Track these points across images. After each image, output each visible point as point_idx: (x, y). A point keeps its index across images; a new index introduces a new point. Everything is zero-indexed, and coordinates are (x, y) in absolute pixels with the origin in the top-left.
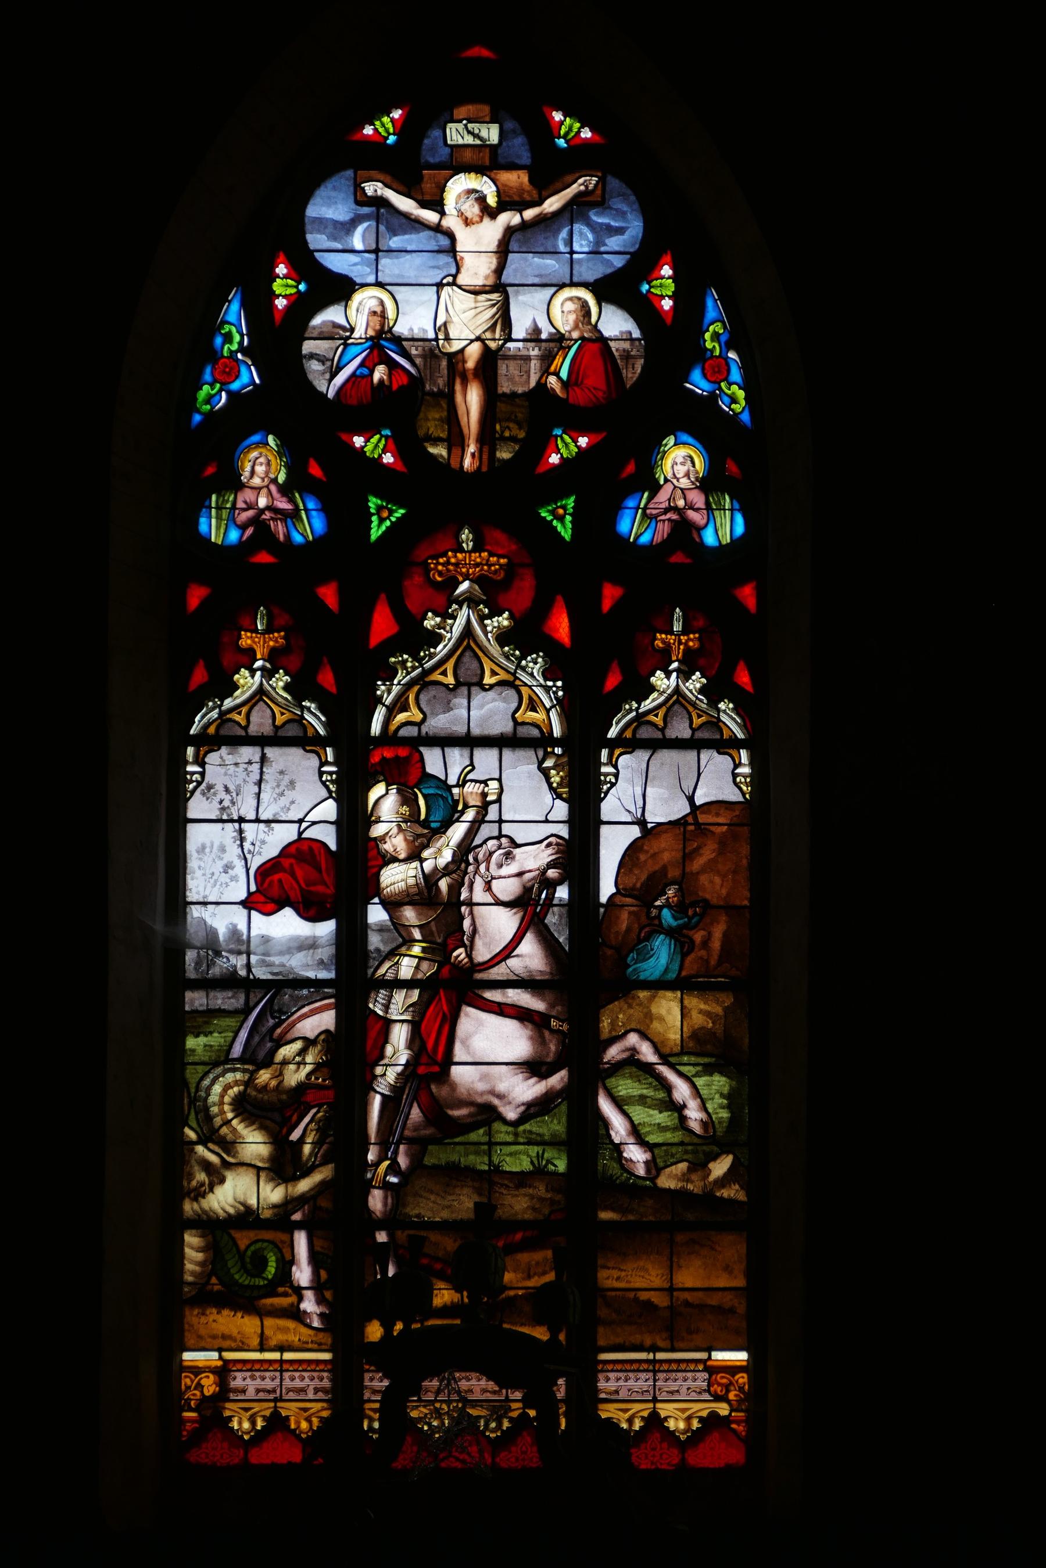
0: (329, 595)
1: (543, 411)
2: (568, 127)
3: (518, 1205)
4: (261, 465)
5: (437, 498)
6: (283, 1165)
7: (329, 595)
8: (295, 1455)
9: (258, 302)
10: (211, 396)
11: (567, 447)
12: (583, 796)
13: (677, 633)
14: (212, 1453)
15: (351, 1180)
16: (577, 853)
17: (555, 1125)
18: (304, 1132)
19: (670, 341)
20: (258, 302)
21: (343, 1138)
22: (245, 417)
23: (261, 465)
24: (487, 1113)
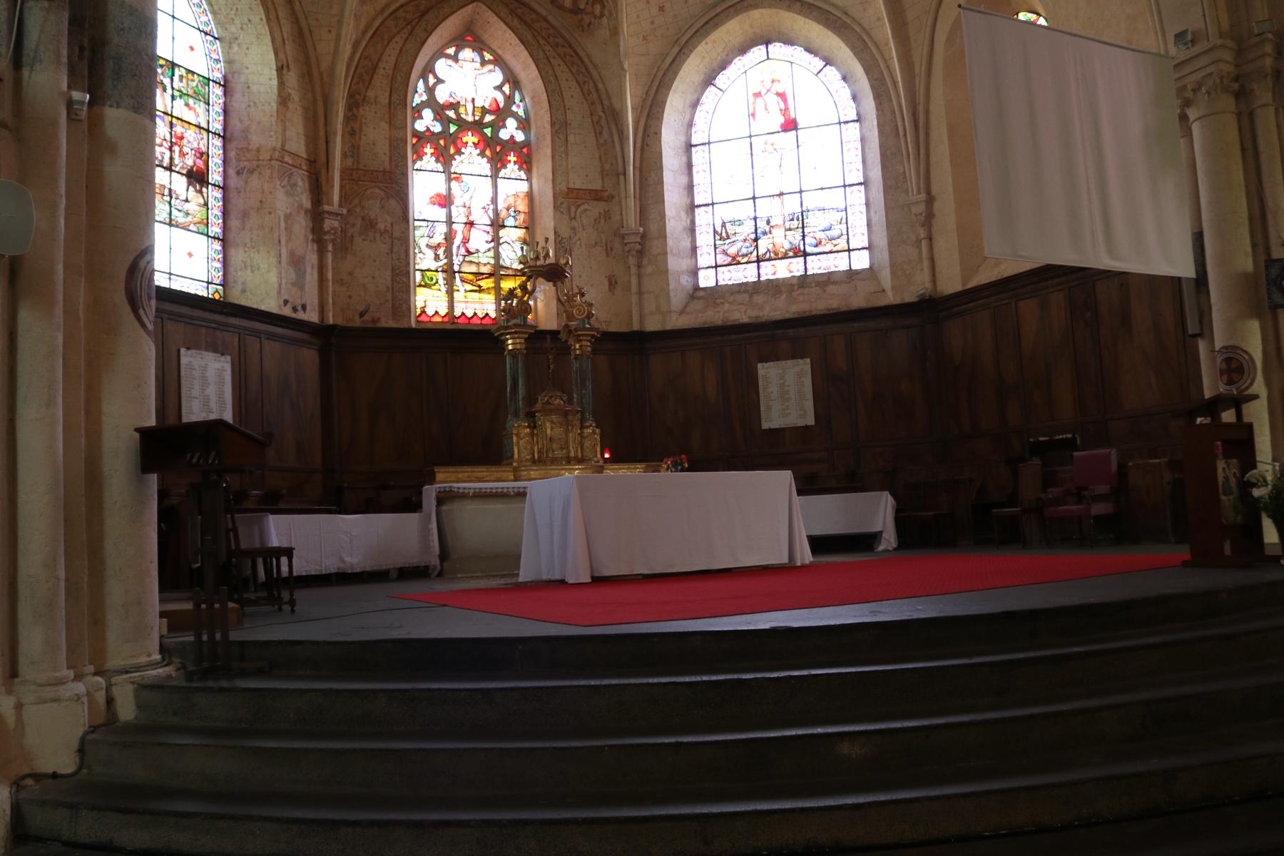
0: (442, 142)
1: (484, 111)
2: (488, 56)
3: (485, 270)
4: (428, 114)
5: (463, 125)
6: (437, 258)
7: (442, 142)
8: (439, 319)
9: (426, 82)
10: (417, 100)
11: (488, 118)
12: (495, 186)
13: (512, 158)
14: (423, 318)
15: (451, 264)
16: (494, 200)
17: (491, 254)
18: (441, 251)
19: (509, 99)
20: (426, 82)
21: (449, 254)
22: (423, 105)
23: (428, 114)
24: (478, 251)
